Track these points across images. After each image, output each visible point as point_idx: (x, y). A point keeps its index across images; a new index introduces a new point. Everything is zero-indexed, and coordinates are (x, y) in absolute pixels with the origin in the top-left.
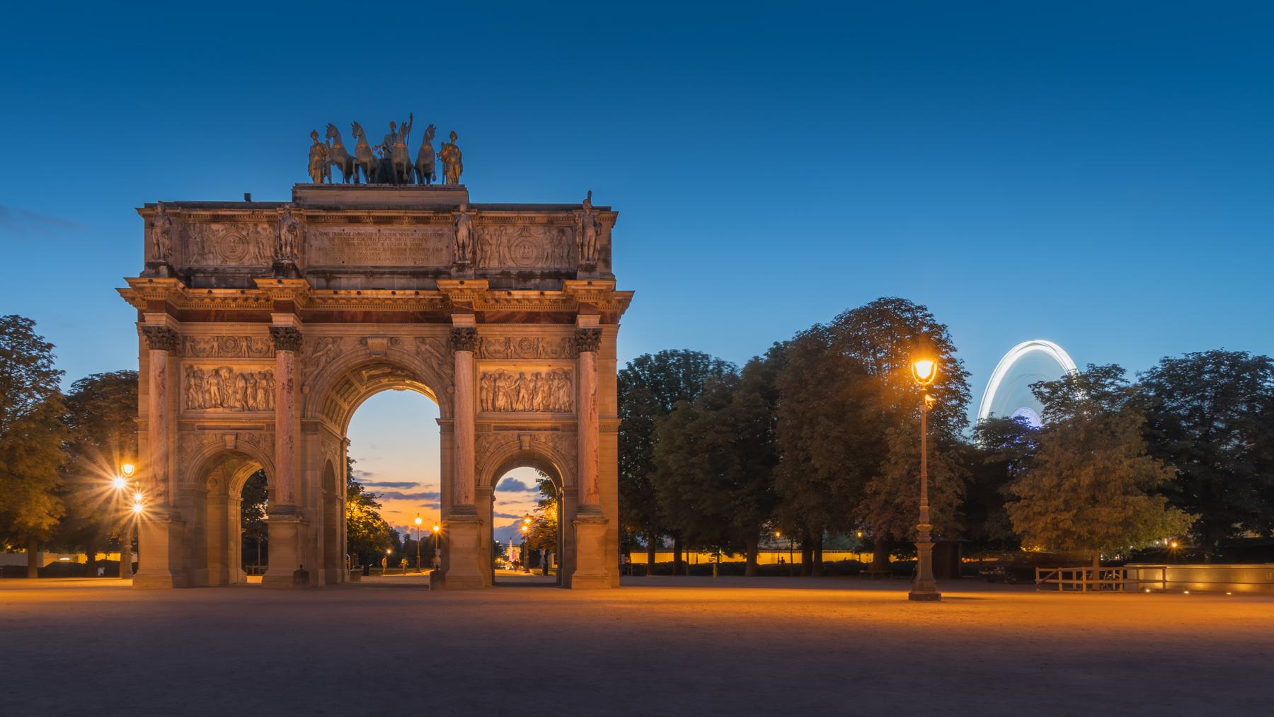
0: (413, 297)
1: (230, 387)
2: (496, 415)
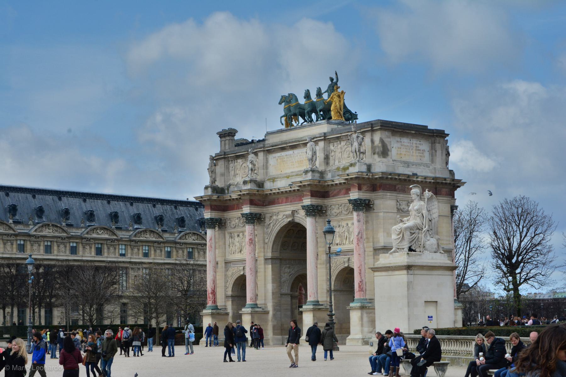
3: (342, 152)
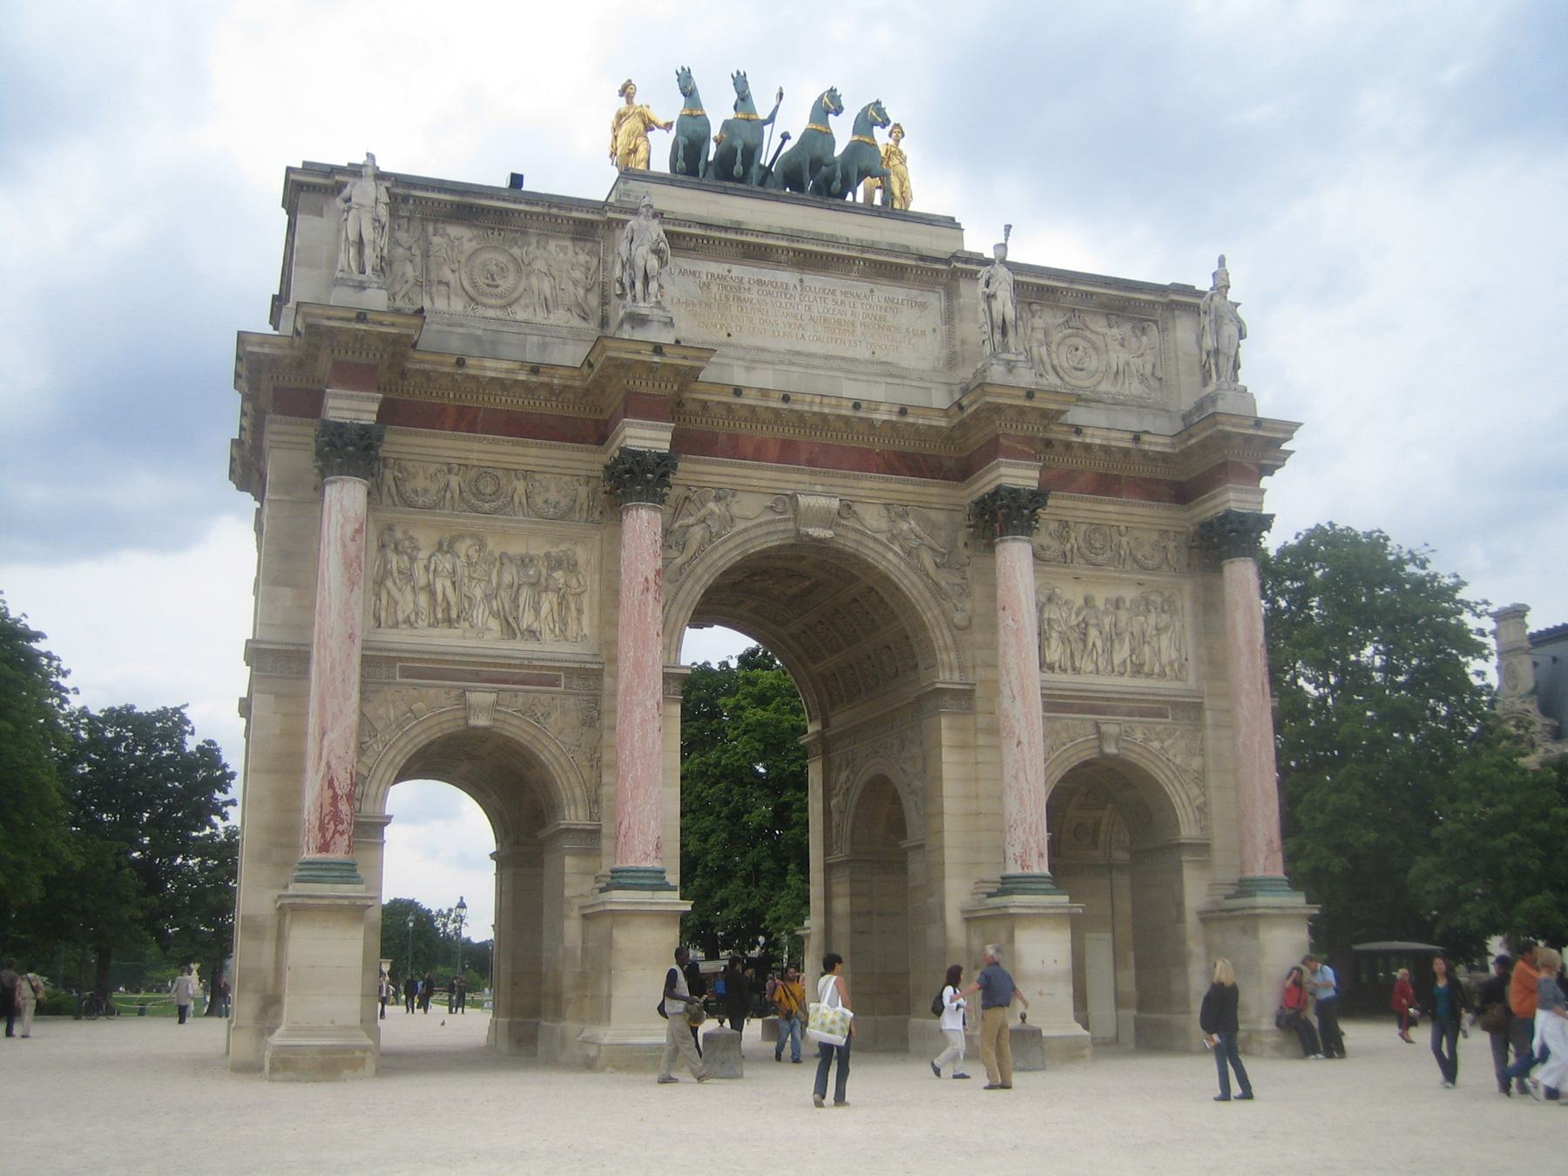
0: (894, 418)
1: (480, 580)
2: (1049, 676)
3: (1048, 345)
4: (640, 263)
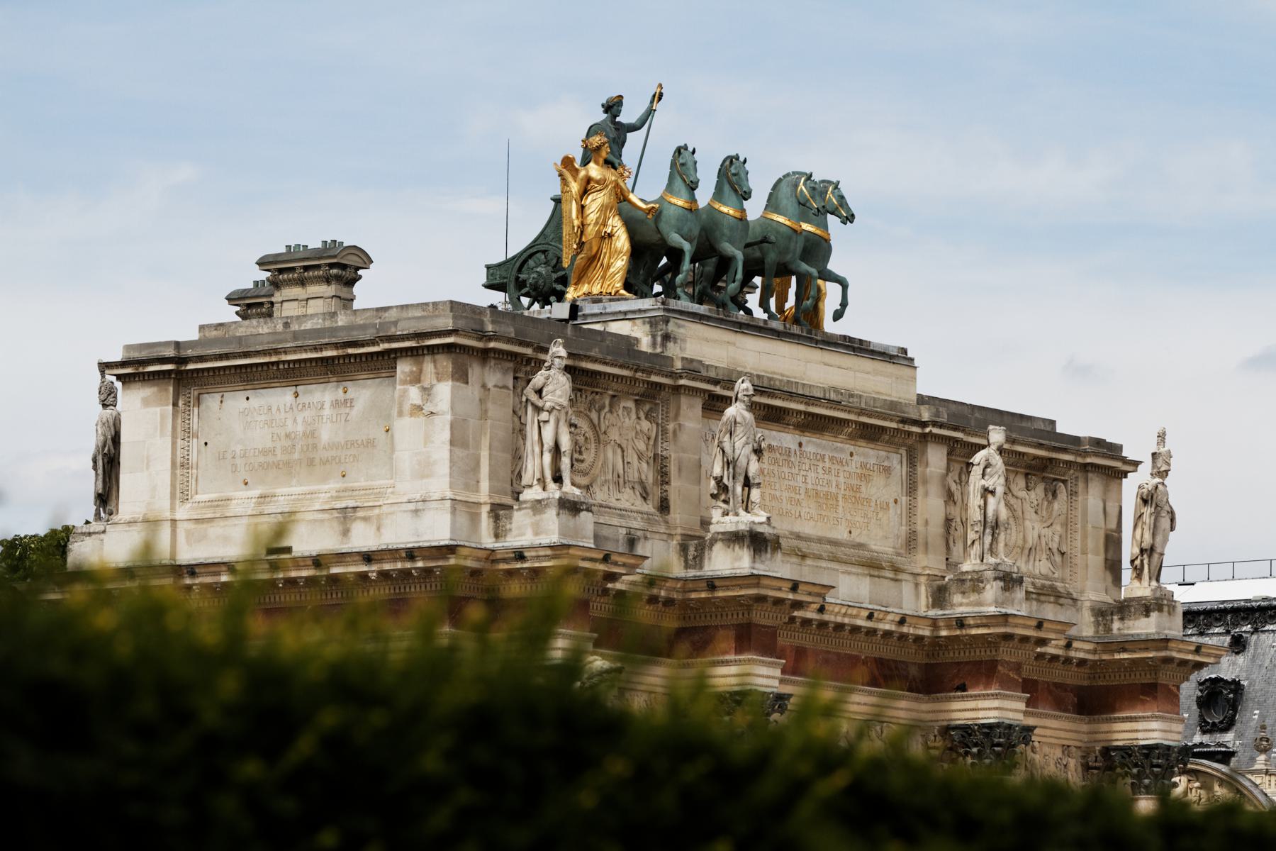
0: (893, 628)
4: (742, 462)
